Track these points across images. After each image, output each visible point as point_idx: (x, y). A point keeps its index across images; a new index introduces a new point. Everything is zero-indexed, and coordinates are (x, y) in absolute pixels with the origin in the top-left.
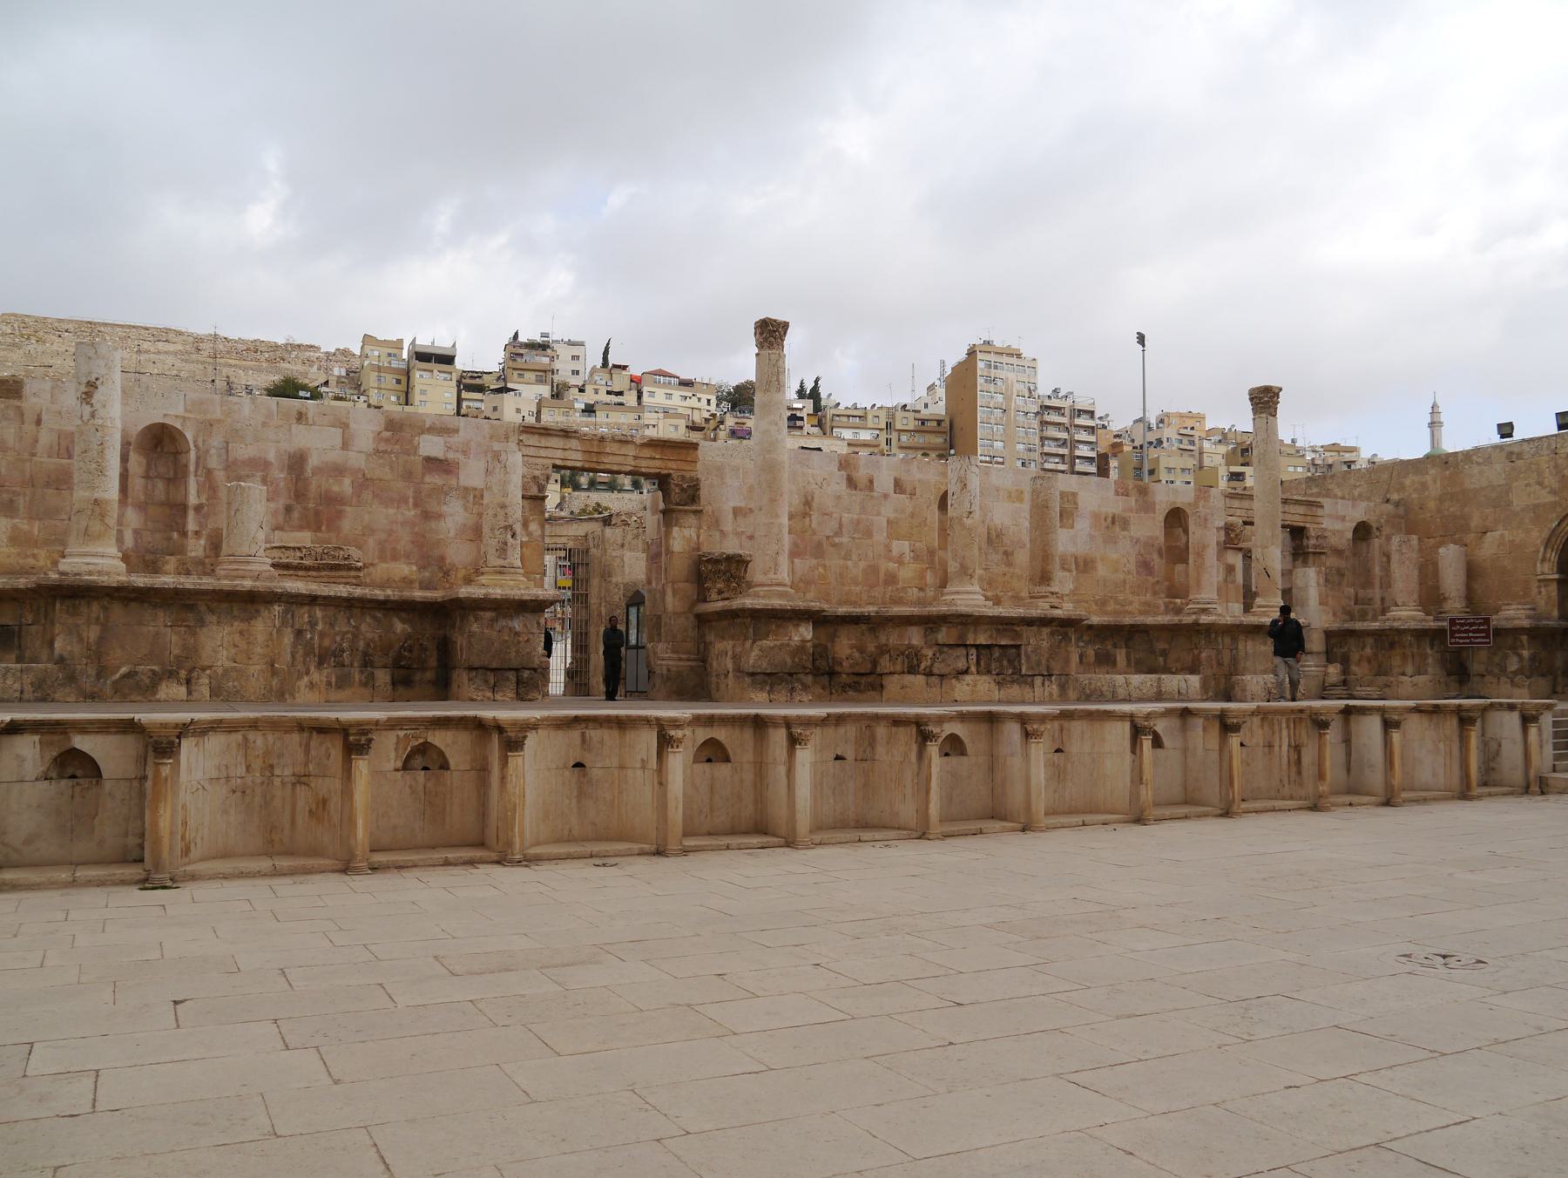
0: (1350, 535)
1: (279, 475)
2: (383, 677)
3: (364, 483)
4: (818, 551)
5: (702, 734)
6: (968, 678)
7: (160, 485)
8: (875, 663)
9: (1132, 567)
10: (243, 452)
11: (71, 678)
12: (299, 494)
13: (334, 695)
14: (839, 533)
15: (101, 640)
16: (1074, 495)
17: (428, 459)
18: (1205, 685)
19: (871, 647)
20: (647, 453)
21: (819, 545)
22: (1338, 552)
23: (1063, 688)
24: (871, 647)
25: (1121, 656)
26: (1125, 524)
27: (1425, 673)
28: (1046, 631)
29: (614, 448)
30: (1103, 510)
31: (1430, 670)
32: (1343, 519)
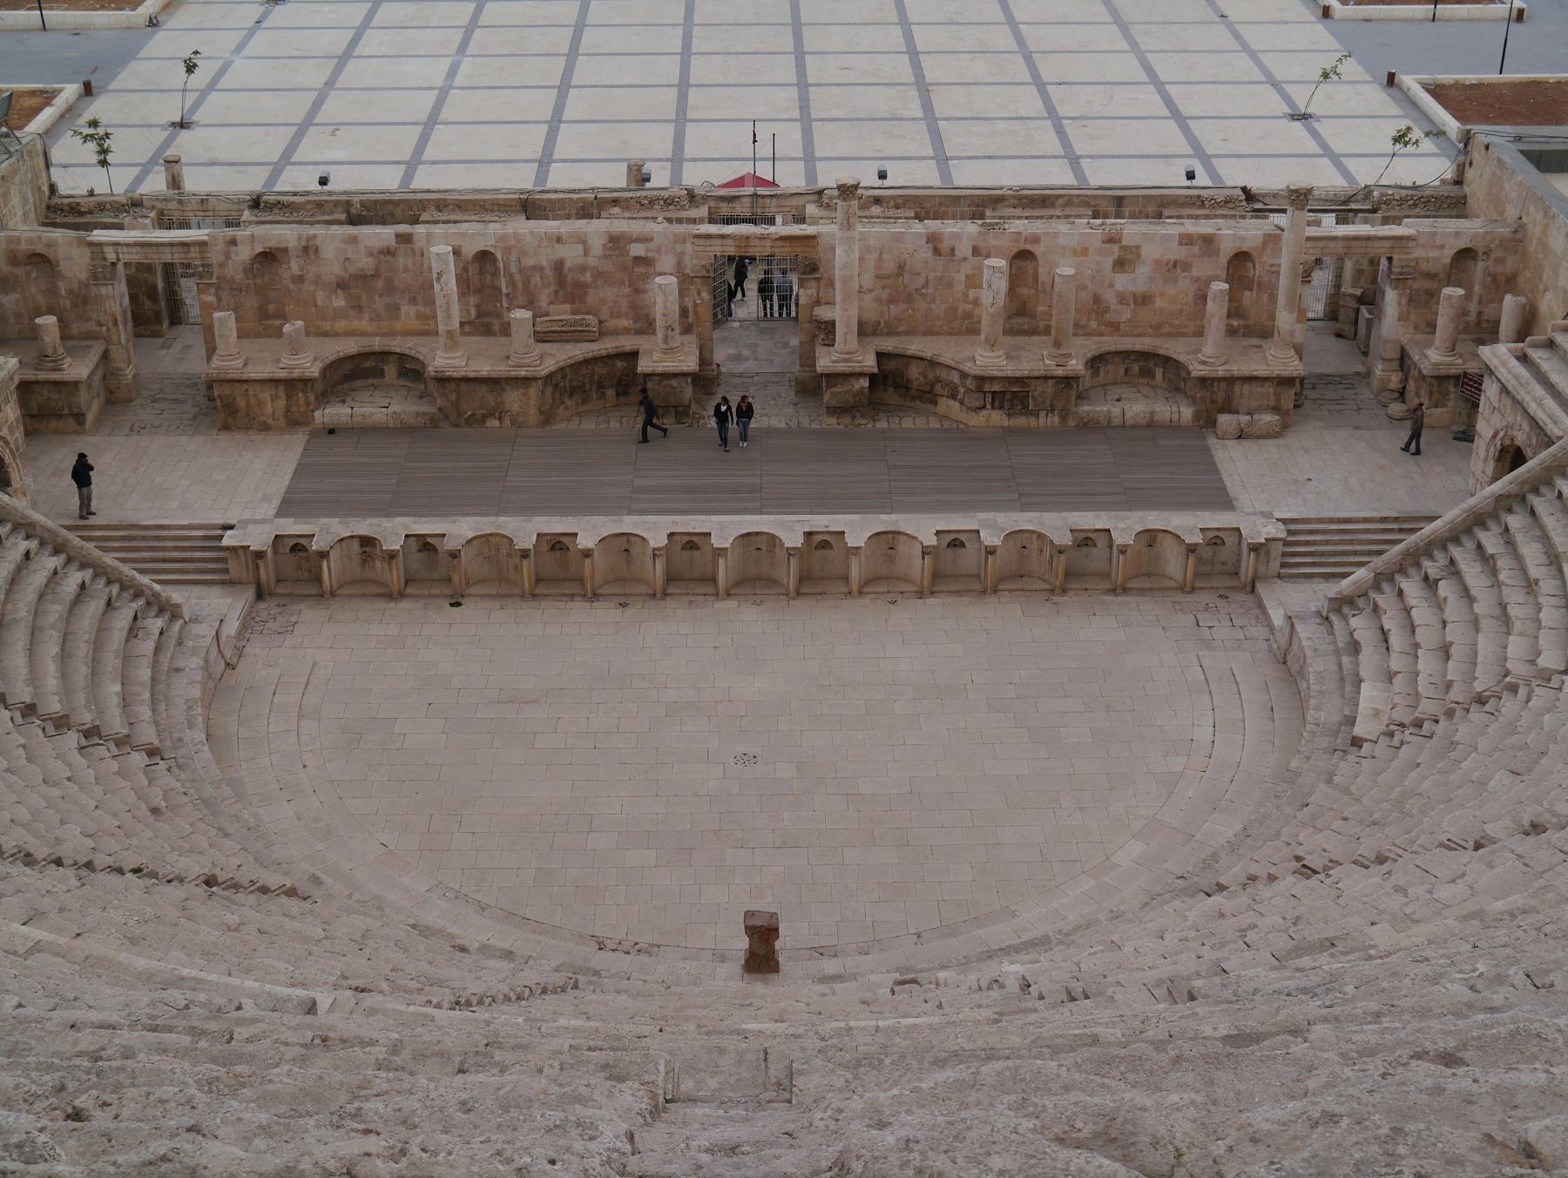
0: (1448, 261)
1: (549, 273)
2: (611, 393)
3: (599, 274)
4: (909, 299)
5: (685, 539)
6: (984, 412)
7: (488, 277)
8: (933, 387)
9: (1190, 299)
10: (529, 262)
11: (446, 417)
12: (561, 282)
13: (581, 409)
14: (926, 285)
15: (457, 399)
16: (1138, 247)
17: (636, 258)
18: (1197, 416)
19: (931, 376)
20: (779, 243)
21: (910, 295)
22: (1430, 276)
23: (1063, 418)
24: (931, 376)
25: (1159, 373)
26: (1186, 267)
27: (1445, 406)
28: (1050, 382)
29: (757, 242)
30: (1166, 257)
31: (1450, 403)
32: (1442, 247)
